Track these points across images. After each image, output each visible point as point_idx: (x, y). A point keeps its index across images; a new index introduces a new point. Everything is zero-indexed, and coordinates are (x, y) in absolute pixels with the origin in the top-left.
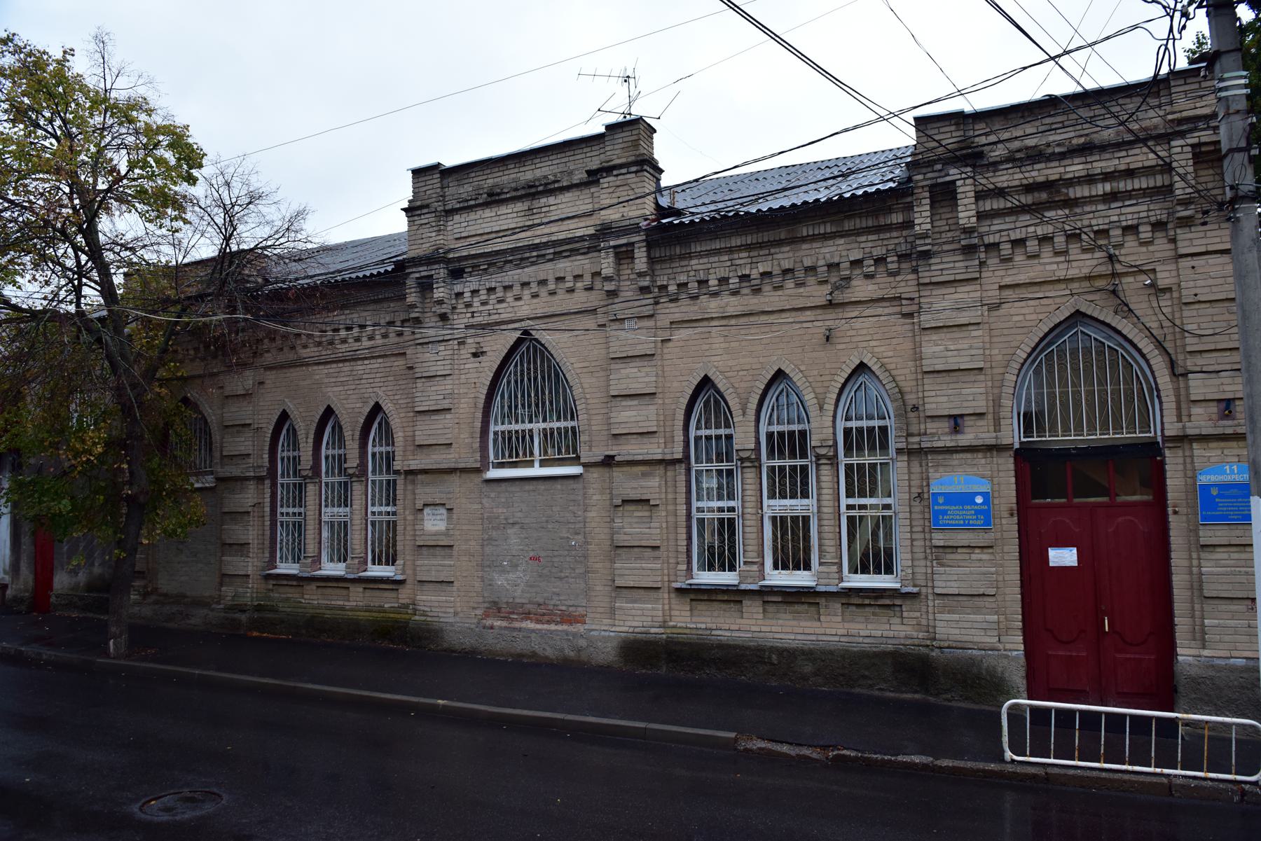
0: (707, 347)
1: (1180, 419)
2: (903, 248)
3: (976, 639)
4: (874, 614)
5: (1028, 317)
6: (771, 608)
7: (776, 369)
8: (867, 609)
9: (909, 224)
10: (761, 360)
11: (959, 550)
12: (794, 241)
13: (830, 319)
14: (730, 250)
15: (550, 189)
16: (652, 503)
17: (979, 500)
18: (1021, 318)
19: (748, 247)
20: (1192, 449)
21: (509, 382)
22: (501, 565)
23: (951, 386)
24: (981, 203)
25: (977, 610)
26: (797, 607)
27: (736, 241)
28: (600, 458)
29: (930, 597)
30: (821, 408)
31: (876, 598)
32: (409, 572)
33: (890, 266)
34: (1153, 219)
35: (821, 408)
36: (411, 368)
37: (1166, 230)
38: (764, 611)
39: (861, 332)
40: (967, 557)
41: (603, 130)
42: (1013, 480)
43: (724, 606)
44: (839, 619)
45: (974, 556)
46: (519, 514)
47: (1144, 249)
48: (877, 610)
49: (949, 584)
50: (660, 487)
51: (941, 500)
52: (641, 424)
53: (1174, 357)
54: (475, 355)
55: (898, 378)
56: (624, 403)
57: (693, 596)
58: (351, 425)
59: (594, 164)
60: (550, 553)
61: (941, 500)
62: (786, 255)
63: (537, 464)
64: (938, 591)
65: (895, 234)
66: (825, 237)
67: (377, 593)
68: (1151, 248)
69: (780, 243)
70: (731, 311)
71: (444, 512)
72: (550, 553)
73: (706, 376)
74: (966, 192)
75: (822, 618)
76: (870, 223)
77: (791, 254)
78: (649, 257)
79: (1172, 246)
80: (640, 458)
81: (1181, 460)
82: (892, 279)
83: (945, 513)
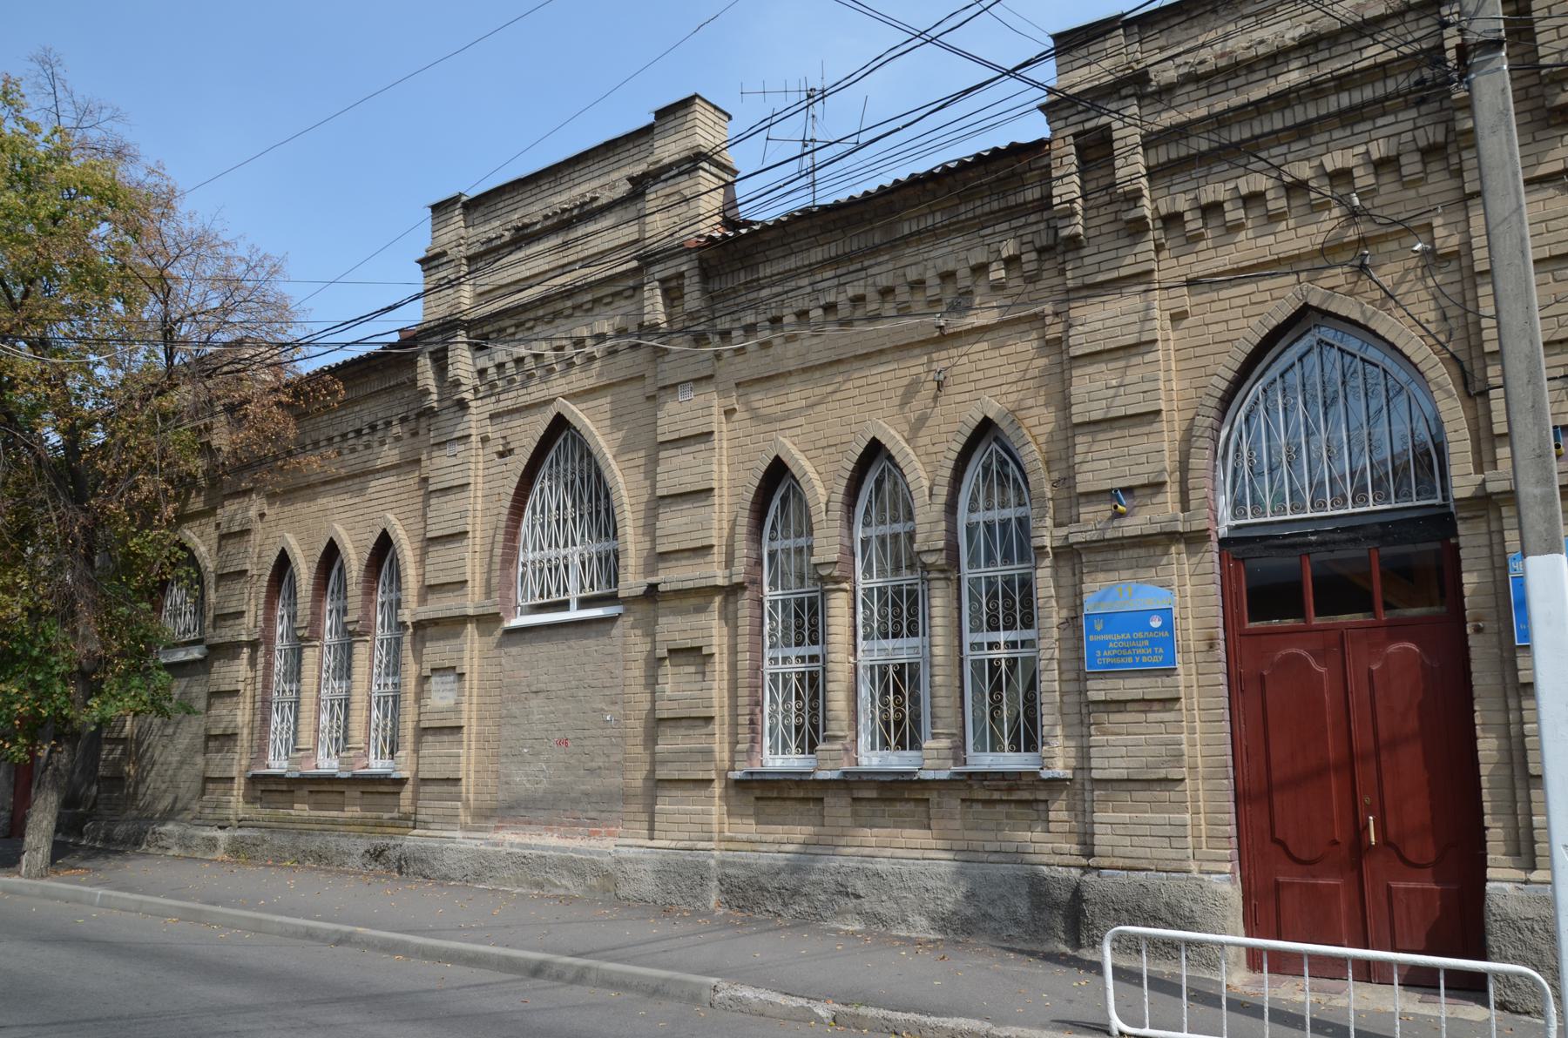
1: (1479, 468)
2: (1044, 240)
3: (1157, 853)
4: (1009, 816)
5: (1232, 325)
6: (865, 809)
8: (999, 808)
9: (1045, 202)
10: (854, 428)
11: (1130, 707)
12: (895, 244)
14: (811, 269)
15: (588, 212)
16: (705, 651)
18: (1223, 326)
20: (1500, 518)
21: (542, 490)
22: (521, 755)
23: (1115, 443)
24: (1152, 152)
25: (1156, 806)
26: (899, 807)
27: (817, 255)
28: (640, 591)
29: (1088, 786)
31: (1010, 789)
33: (1026, 267)
34: (1422, 143)
36: (425, 480)
37: (1447, 158)
38: (855, 814)
39: (989, 373)
41: (651, 119)
42: (1217, 588)
43: (799, 807)
47: (1412, 193)
48: (1013, 809)
51: (1099, 627)
52: (694, 536)
53: (1467, 366)
54: (502, 455)
57: (758, 793)
58: (354, 561)
59: (638, 170)
60: (580, 734)
62: (884, 268)
63: (574, 605)
64: (1096, 774)
65: (1033, 218)
66: (934, 234)
69: (875, 251)
70: (814, 359)
72: (580, 734)
73: (777, 458)
74: (1127, 135)
75: (933, 823)
76: (995, 206)
77: (890, 266)
78: (704, 291)
79: (1454, 183)
80: (690, 585)
81: (1484, 540)
82: (1030, 287)
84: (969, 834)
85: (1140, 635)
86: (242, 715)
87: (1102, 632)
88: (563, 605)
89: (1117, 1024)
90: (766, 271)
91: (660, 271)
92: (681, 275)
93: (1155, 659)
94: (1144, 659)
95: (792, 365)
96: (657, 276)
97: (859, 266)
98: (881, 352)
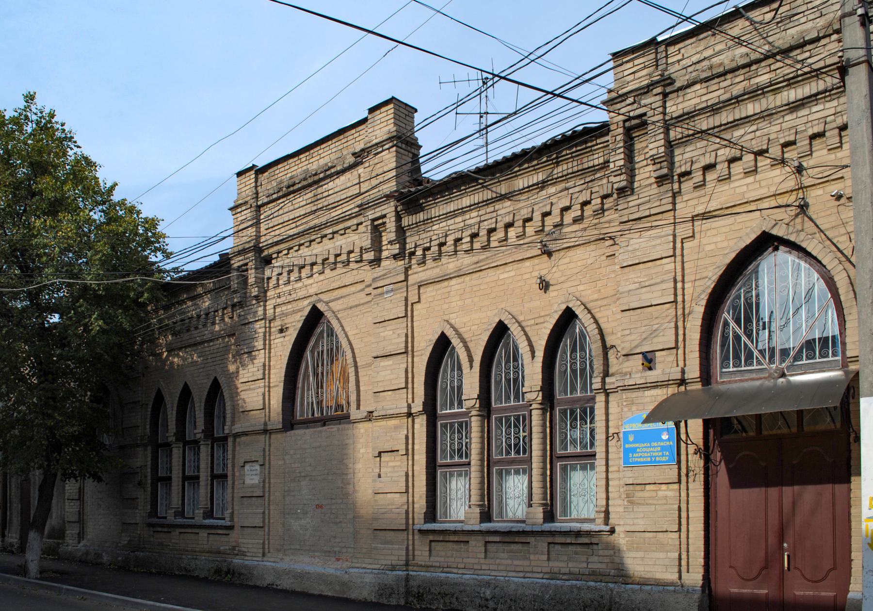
0: (446, 306)
7: (497, 320)
13: (543, 267)
17: (665, 437)
25: (662, 547)
30: (533, 357)
32: (236, 520)
35: (533, 357)
40: (654, 494)
44: (545, 557)
45: (660, 493)
46: (309, 468)
49: (636, 521)
50: (407, 437)
51: (631, 439)
55: (600, 321)
56: (382, 364)
61: (631, 439)
67: (217, 537)
71: (258, 467)
80: (391, 412)
83: (634, 450)
85: (655, 444)
87: (631, 443)
90: (435, 212)
91: (371, 214)
92: (384, 216)
93: (664, 459)
94: (657, 459)
96: (371, 217)
97: (492, 209)
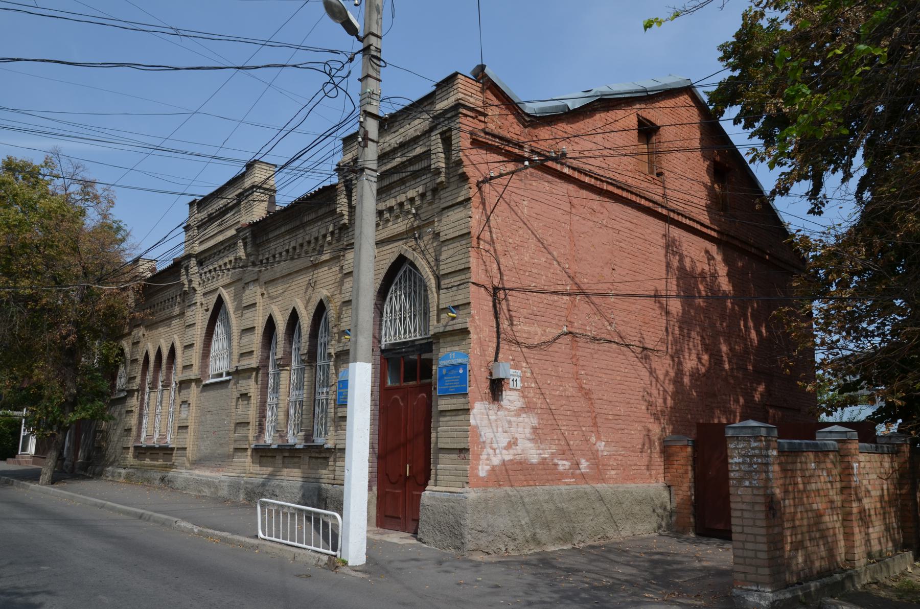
6: (286, 460)
8: (319, 460)
12: (303, 226)
19: (289, 232)
27: (283, 230)
31: (320, 452)
38: (283, 463)
68: (434, 206)
69: (297, 228)
70: (285, 272)
84: (310, 471)
86: (133, 421)
88: (221, 375)
89: (261, 535)
90: (271, 236)
95: (278, 275)
98: (301, 270)
